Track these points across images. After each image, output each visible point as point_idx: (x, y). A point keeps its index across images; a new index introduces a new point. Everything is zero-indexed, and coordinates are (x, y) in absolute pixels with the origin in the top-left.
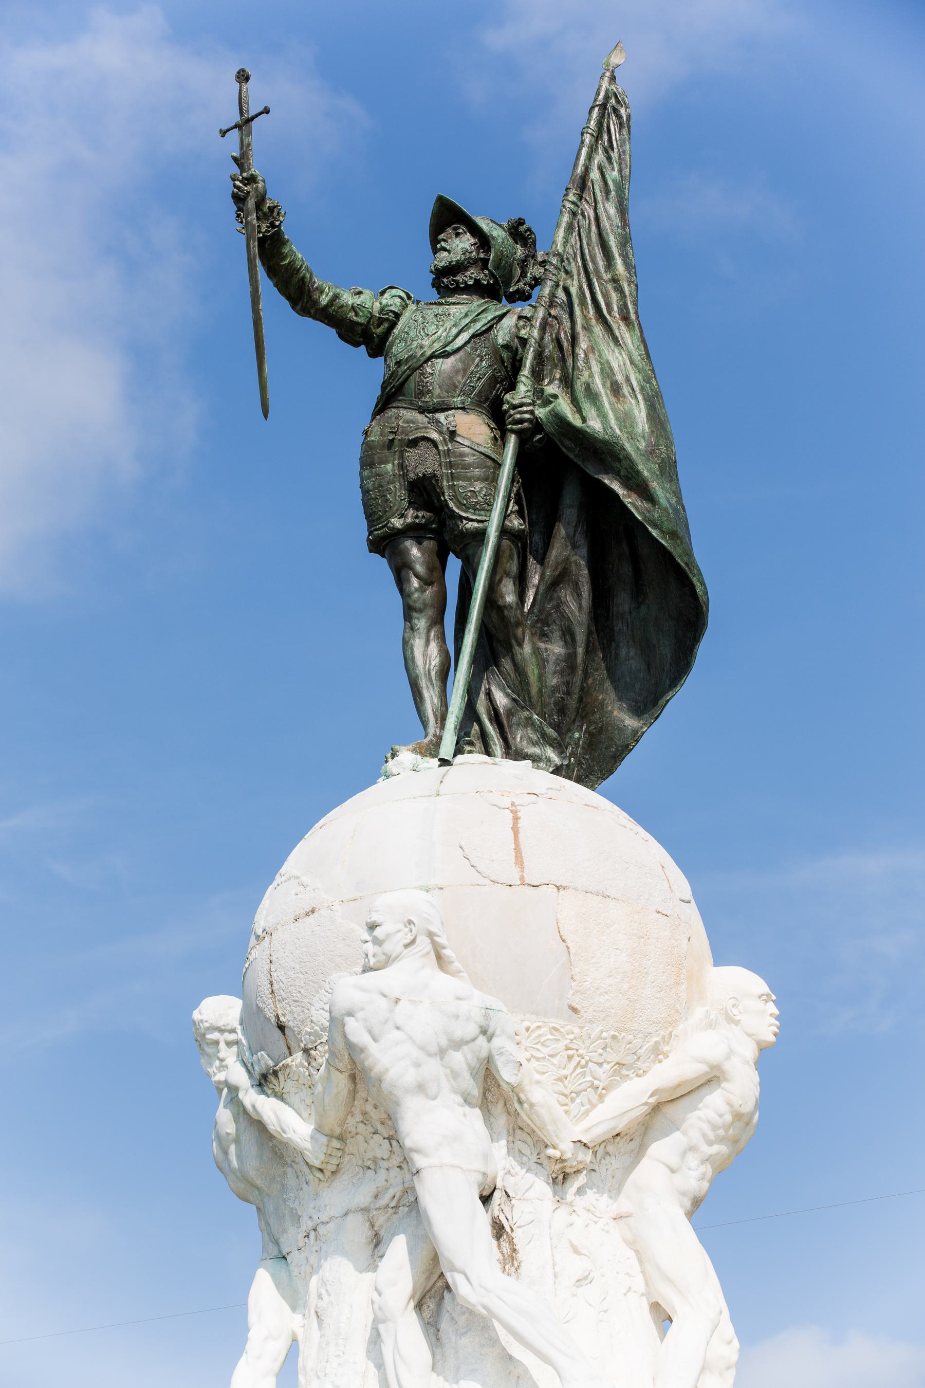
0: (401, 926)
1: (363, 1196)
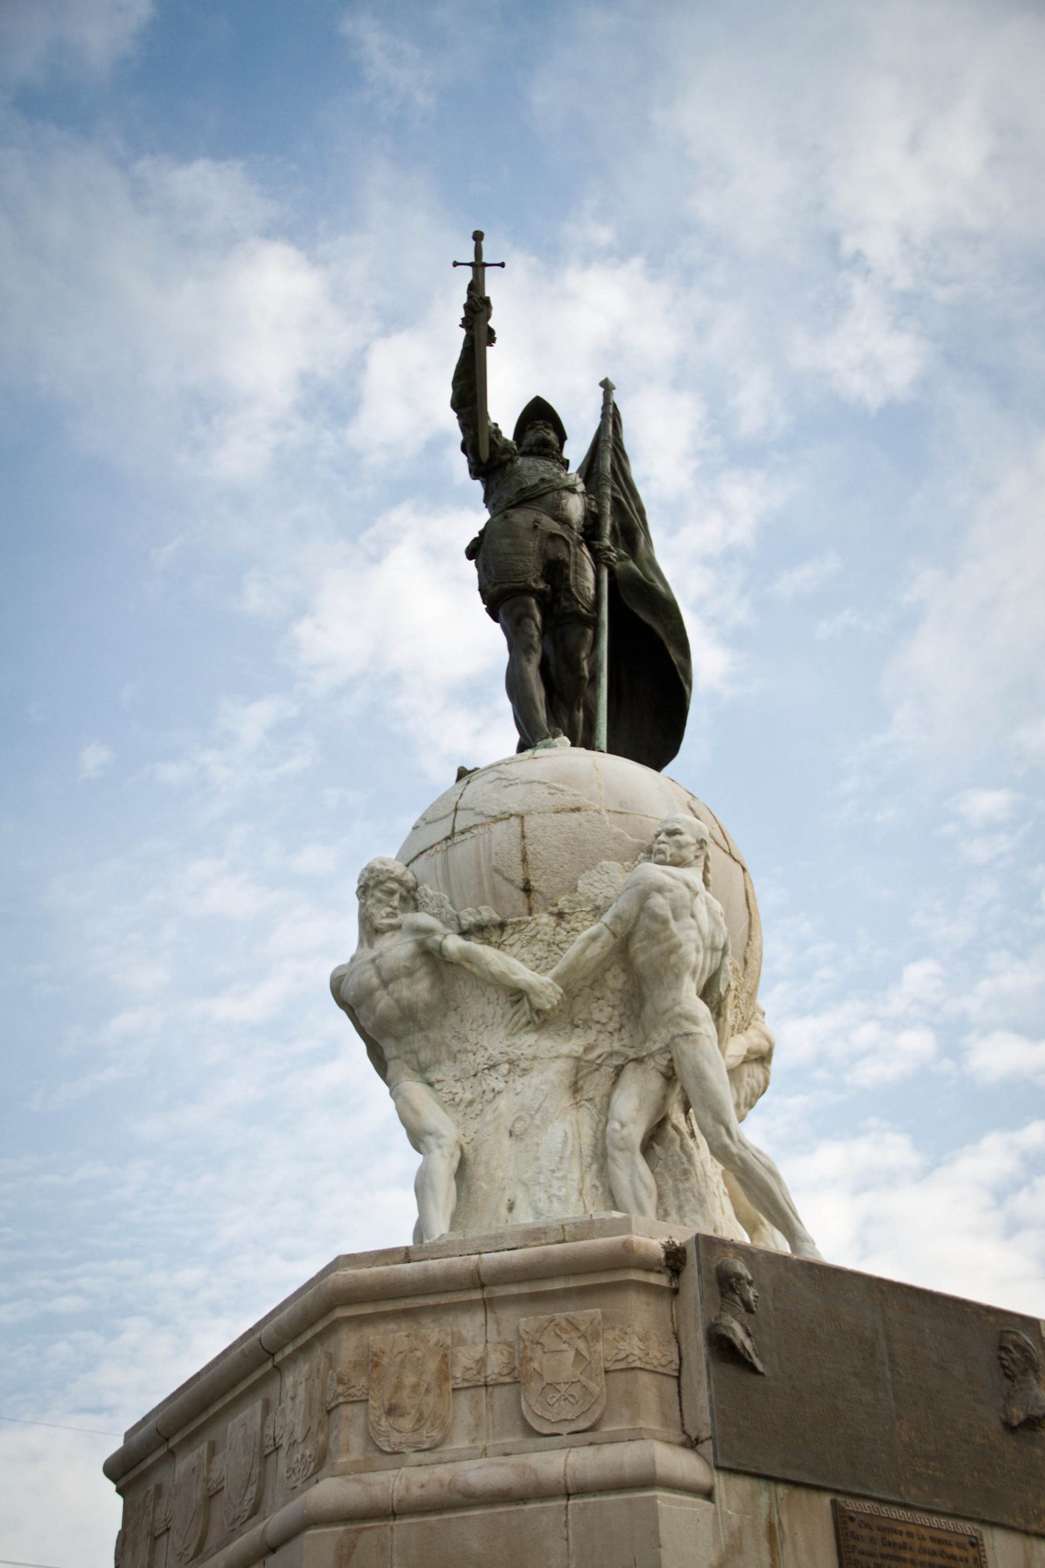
0: (694, 841)
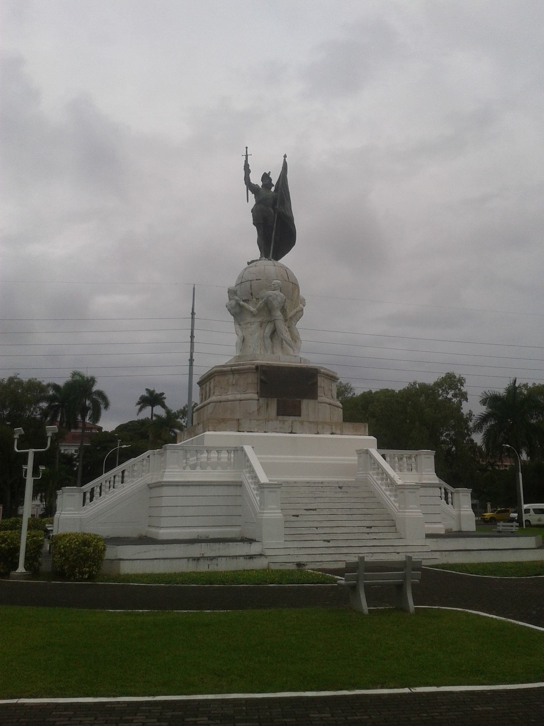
1: (260, 319)
